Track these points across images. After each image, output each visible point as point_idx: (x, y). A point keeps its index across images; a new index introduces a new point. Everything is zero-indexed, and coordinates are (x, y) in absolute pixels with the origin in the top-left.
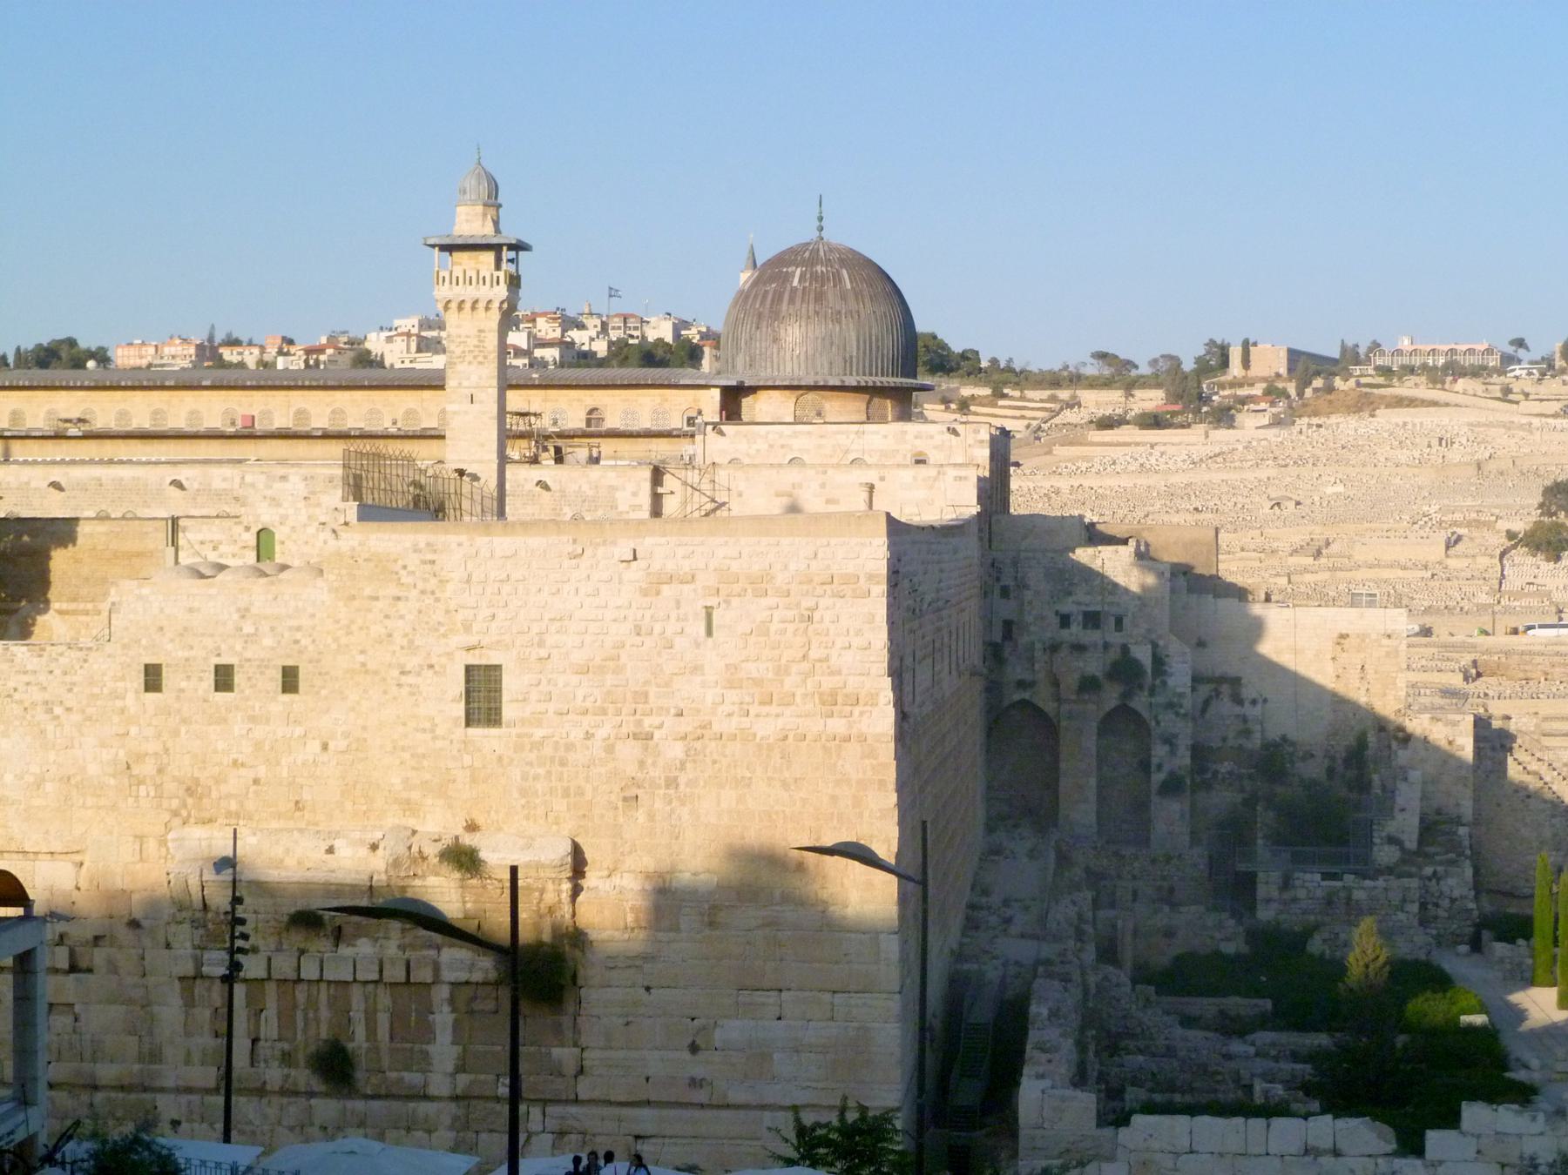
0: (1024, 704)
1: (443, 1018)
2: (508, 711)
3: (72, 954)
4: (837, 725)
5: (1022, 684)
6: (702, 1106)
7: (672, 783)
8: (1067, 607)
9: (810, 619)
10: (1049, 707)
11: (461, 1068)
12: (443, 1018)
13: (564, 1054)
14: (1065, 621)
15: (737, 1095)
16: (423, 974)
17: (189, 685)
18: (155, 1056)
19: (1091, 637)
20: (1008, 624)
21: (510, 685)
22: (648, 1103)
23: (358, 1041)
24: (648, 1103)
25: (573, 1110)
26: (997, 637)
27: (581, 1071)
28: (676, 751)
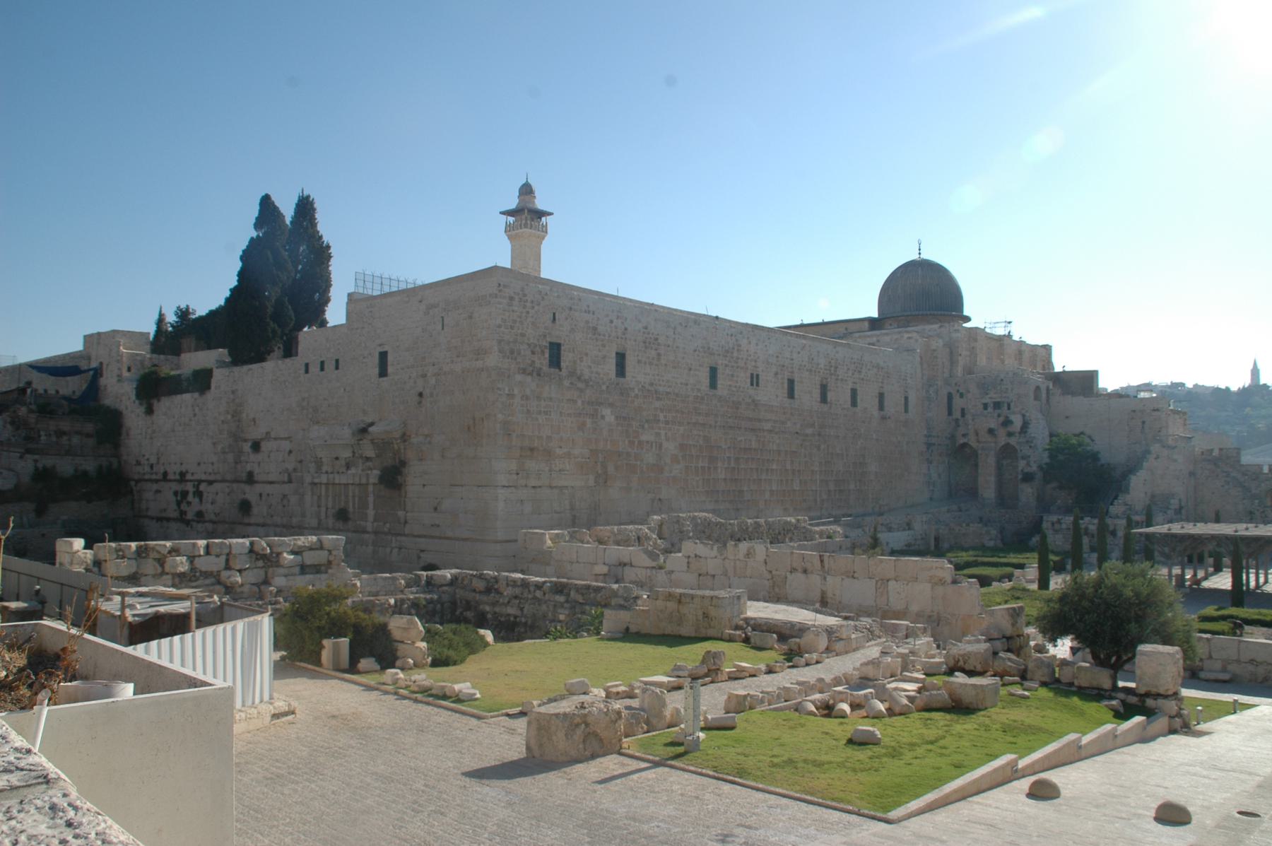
0: (964, 445)
1: (371, 499)
2: (390, 370)
3: (289, 475)
4: (479, 364)
5: (964, 435)
6: (440, 538)
7: (432, 395)
8: (985, 401)
9: (471, 317)
10: (973, 444)
11: (375, 520)
12: (371, 499)
13: (401, 513)
14: (985, 406)
15: (449, 534)
16: (364, 481)
17: (315, 369)
18: (303, 515)
19: (998, 411)
20: (963, 410)
21: (390, 358)
22: (425, 536)
23: (351, 509)
24: (425, 536)
25: (403, 538)
26: (957, 414)
27: (406, 522)
28: (433, 381)
